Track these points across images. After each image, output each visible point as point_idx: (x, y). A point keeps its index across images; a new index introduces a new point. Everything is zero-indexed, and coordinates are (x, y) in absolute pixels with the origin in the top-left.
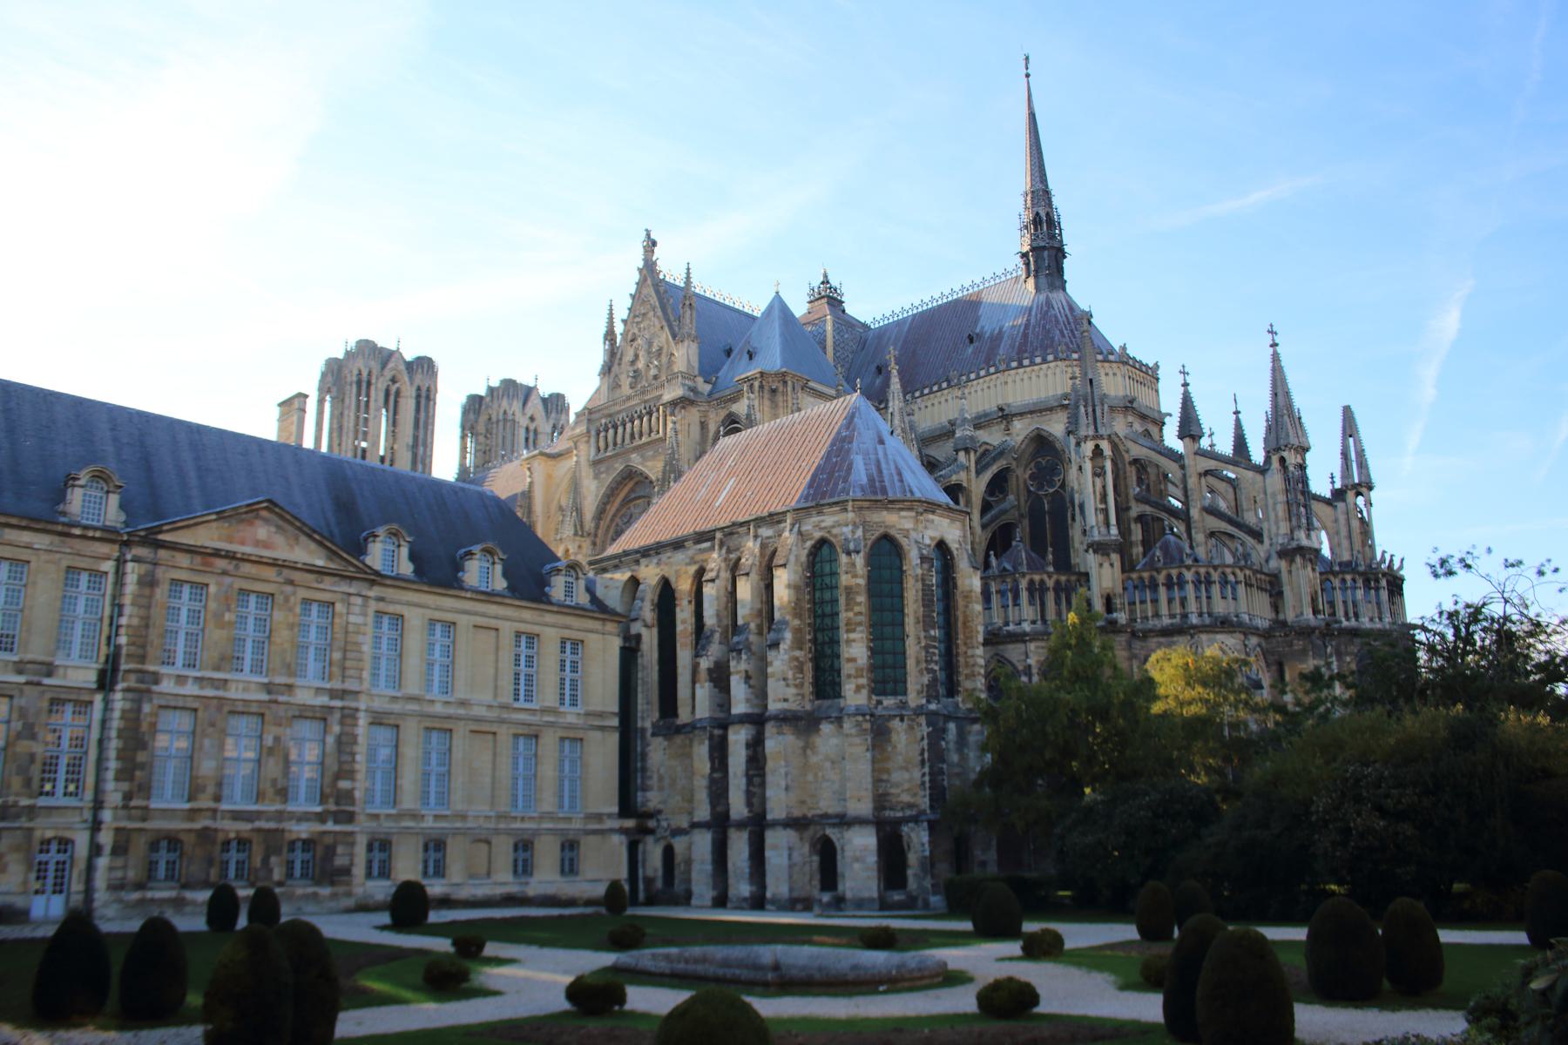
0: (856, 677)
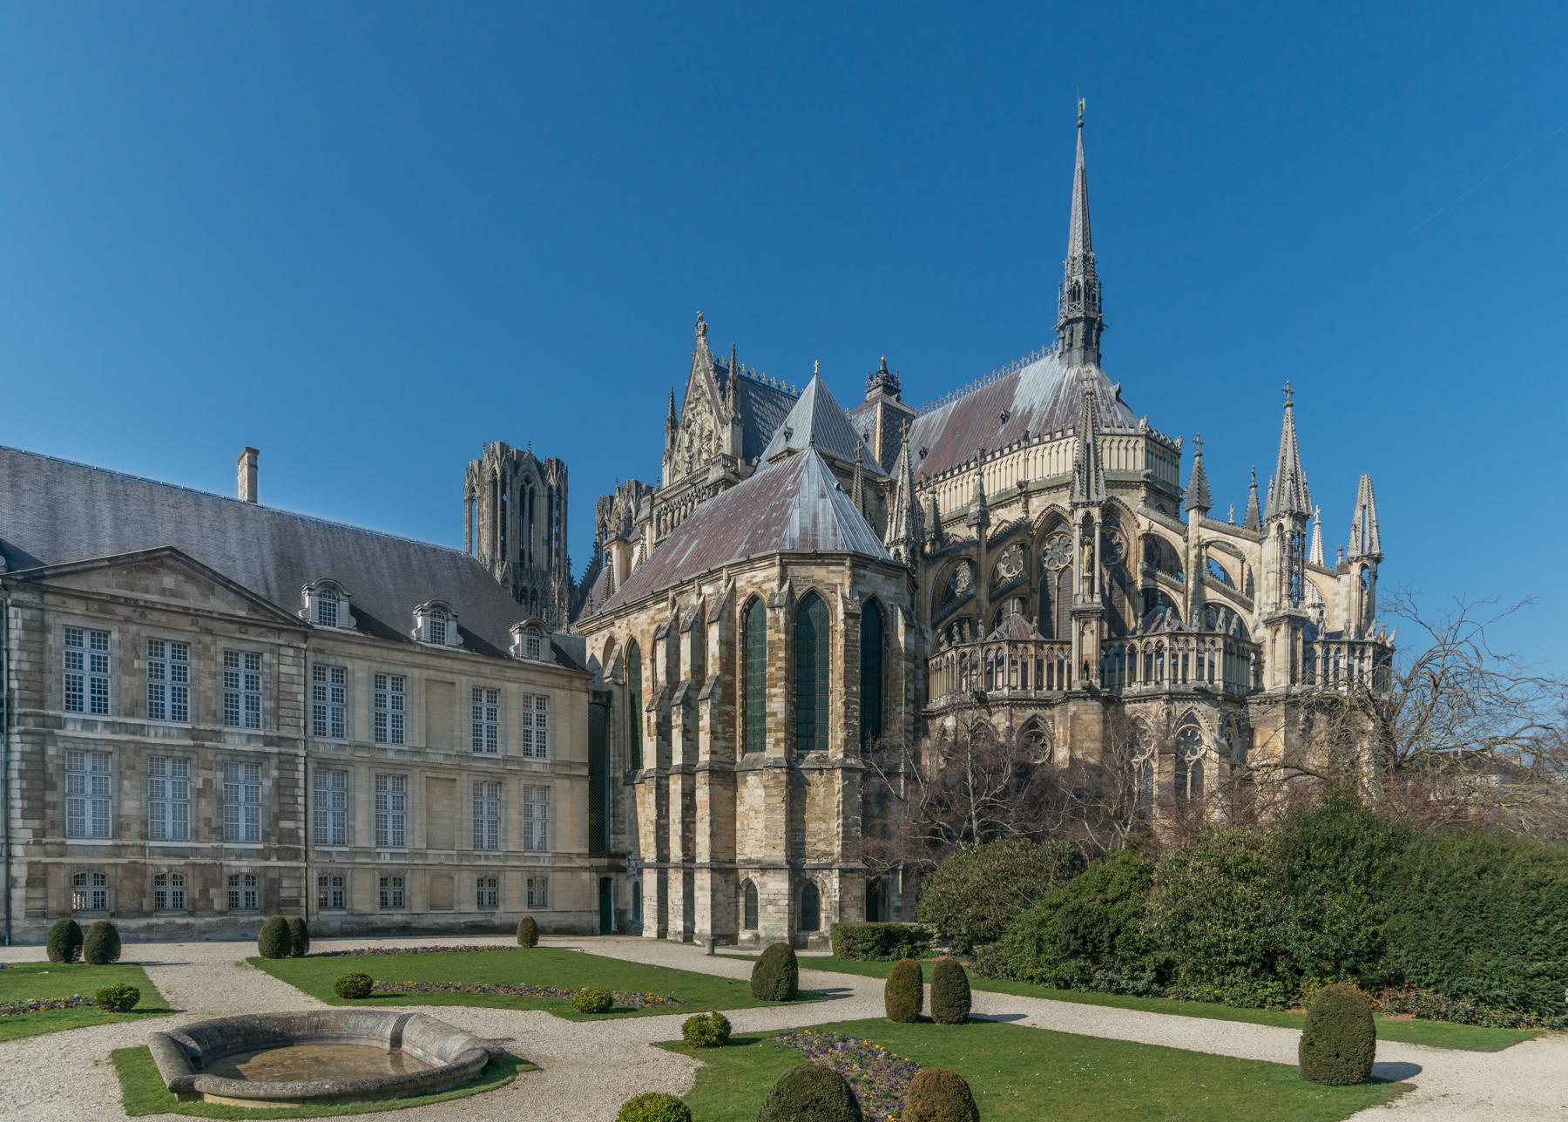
0: (775, 731)
